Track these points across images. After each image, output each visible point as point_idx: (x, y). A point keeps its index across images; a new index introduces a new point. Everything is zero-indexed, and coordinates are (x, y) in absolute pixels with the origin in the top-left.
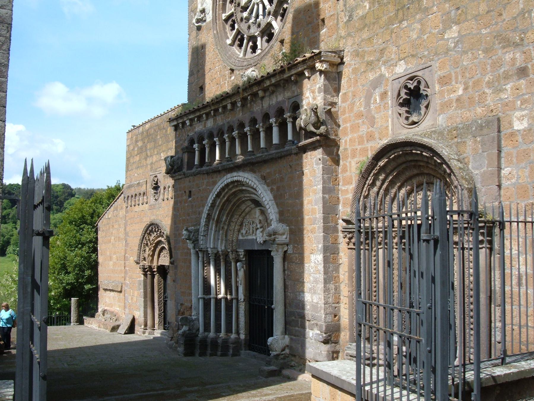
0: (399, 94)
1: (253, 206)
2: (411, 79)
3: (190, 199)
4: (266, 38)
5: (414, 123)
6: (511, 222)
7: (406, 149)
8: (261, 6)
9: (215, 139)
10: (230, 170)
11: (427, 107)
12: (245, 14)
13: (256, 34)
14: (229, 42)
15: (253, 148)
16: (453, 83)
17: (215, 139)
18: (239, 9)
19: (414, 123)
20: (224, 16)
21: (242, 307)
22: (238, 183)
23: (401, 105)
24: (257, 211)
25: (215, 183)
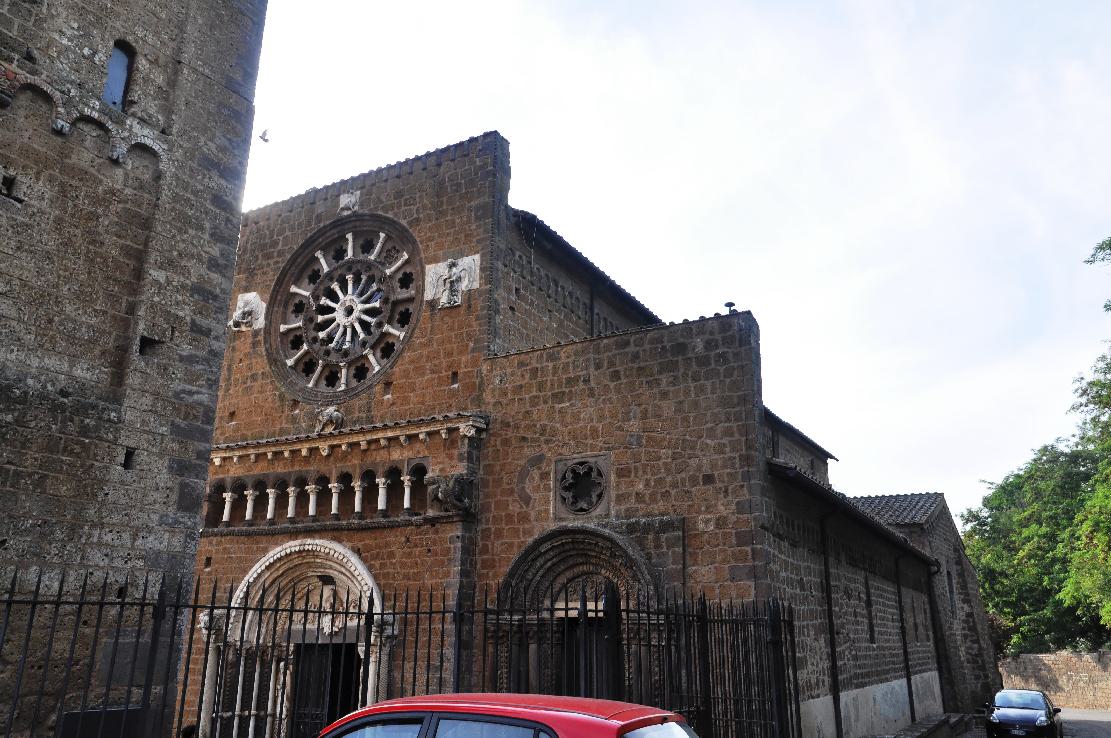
0: (564, 477)
1: (320, 583)
2: (581, 464)
3: (207, 570)
4: (352, 371)
5: (582, 510)
6: (711, 621)
7: (577, 536)
8: (349, 331)
9: (268, 491)
10: (294, 534)
11: (600, 496)
12: (322, 335)
13: (341, 364)
14: (290, 362)
15: (338, 509)
16: (633, 475)
17: (268, 491)
18: (312, 326)
19: (582, 510)
20: (283, 328)
21: (284, 722)
22: (313, 553)
23: (566, 489)
24: (327, 591)
25: (265, 551)
